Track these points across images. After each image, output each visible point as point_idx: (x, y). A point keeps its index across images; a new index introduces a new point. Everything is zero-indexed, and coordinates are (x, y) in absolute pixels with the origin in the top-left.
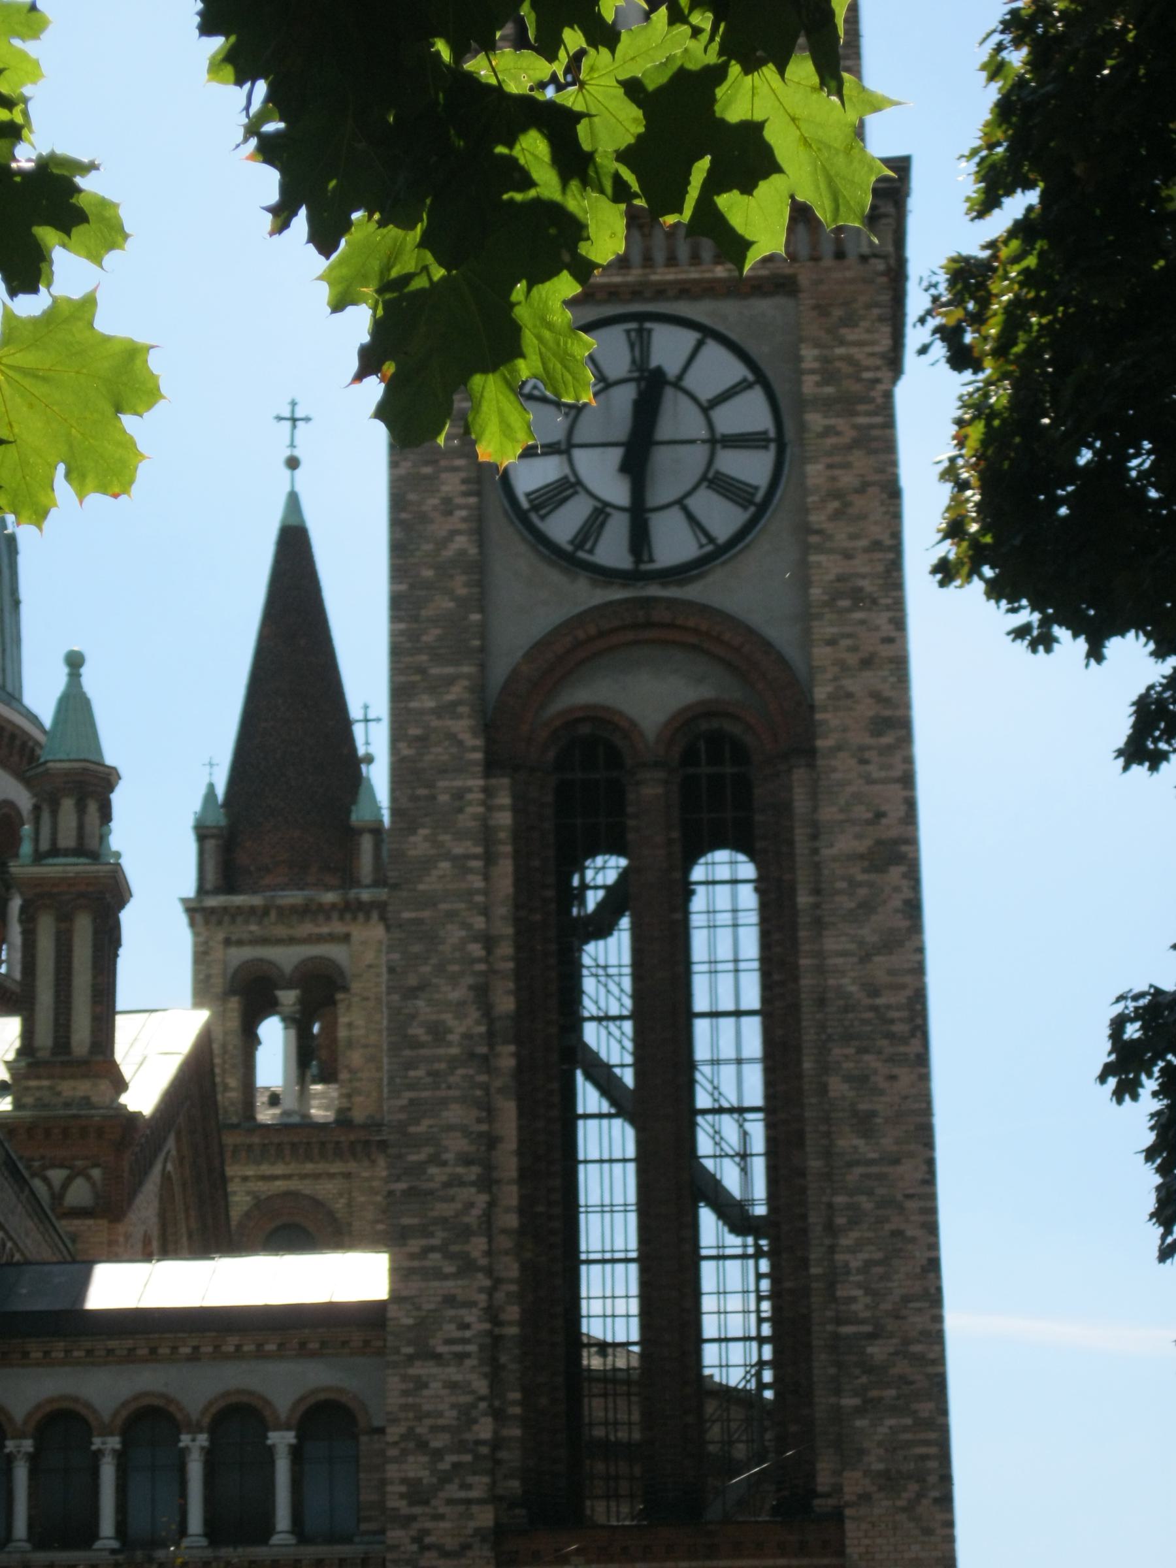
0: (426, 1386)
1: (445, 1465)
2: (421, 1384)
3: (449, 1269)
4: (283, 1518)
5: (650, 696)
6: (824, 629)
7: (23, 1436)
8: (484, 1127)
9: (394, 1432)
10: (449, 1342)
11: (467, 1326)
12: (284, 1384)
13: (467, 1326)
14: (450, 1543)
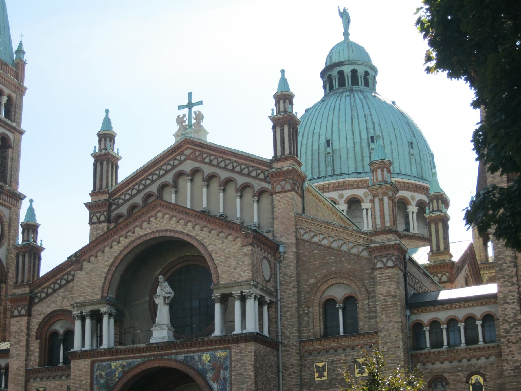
0: (506, 309)
1: (512, 325)
2: (505, 309)
3: (509, 285)
4: (481, 339)
7: (427, 326)
8: (514, 255)
9: (501, 319)
10: (511, 300)
11: (514, 296)
12: (478, 311)
13: (514, 296)
14: (514, 341)
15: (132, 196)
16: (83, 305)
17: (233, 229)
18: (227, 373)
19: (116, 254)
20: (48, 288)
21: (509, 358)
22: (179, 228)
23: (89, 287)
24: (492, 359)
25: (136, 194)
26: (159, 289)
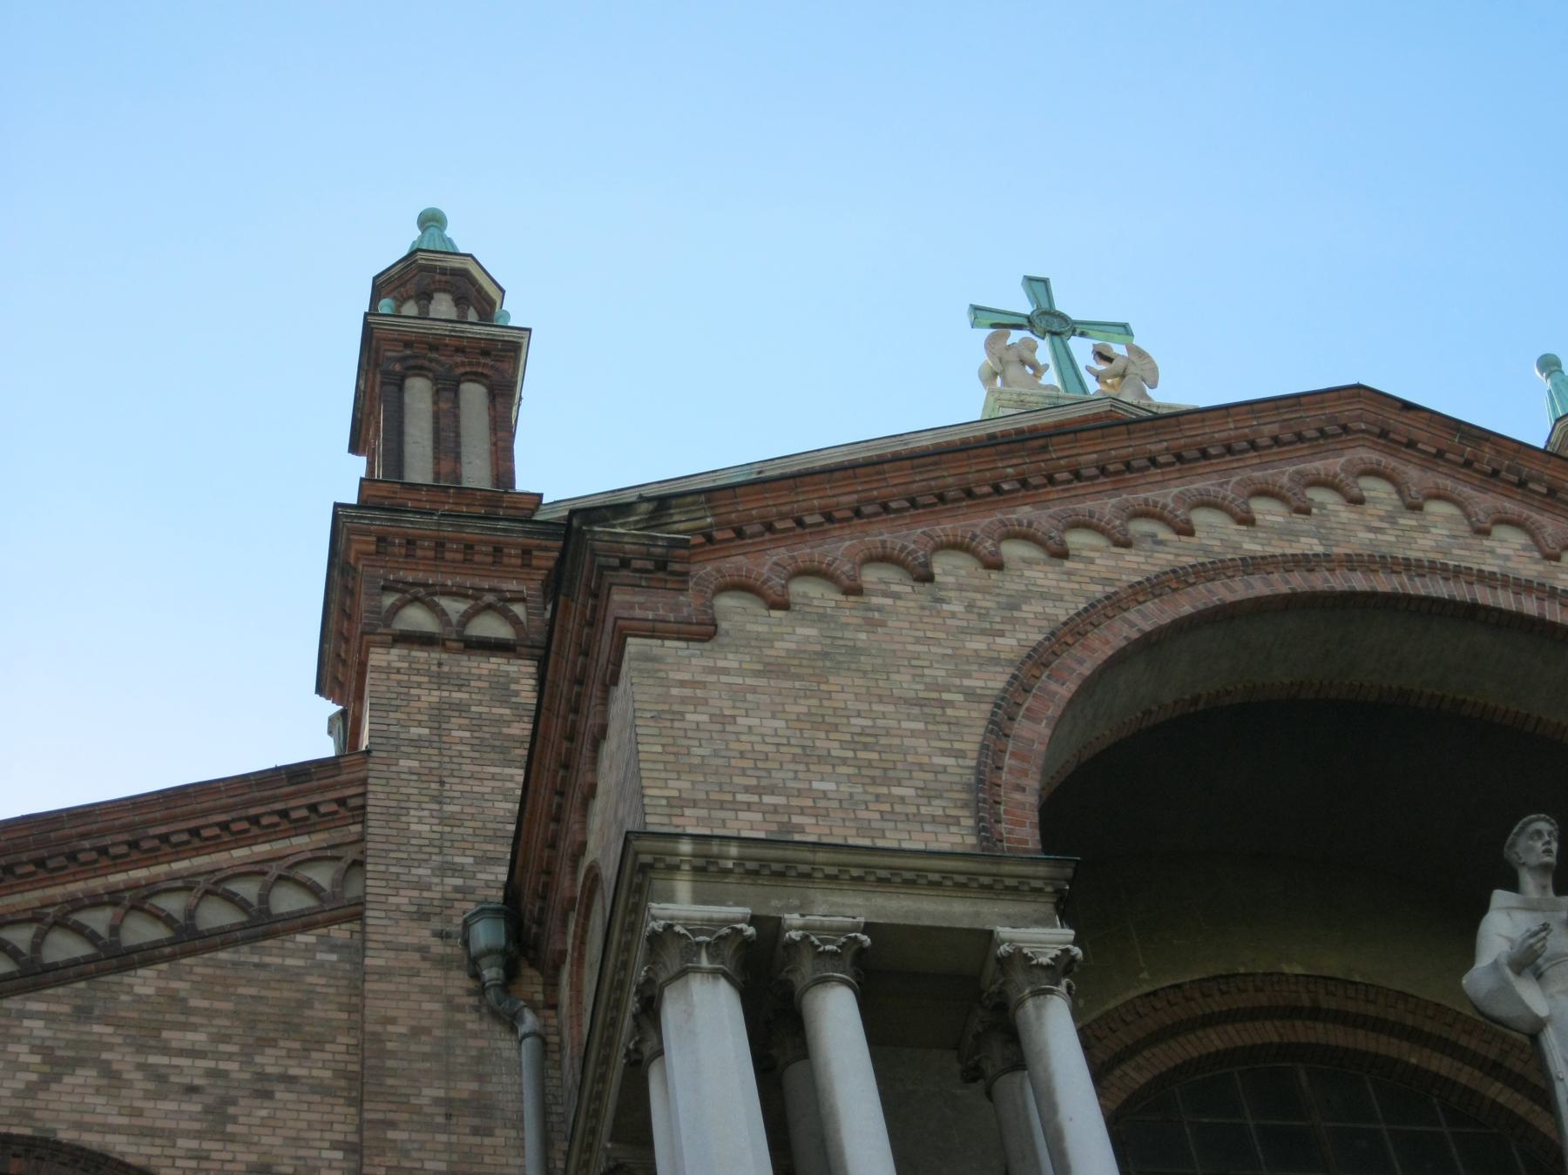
16: (779, 862)
23: (808, 757)
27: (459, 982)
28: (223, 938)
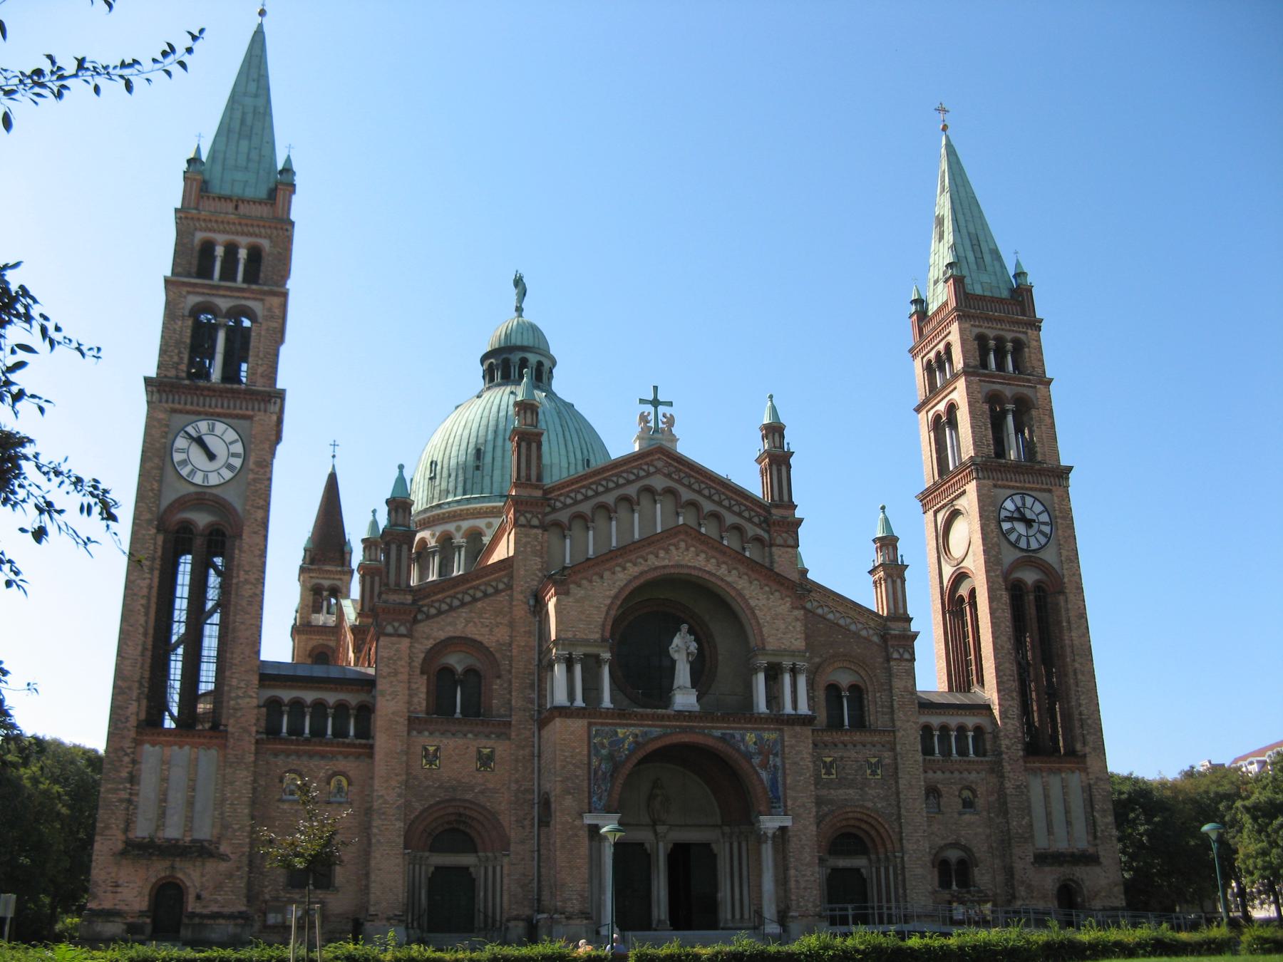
5: (1030, 577)
6: (1065, 566)
15: (576, 502)
17: (782, 585)
18: (778, 761)
19: (622, 584)
20: (442, 601)
21: (1011, 775)
22: (710, 567)
24: (983, 775)
25: (582, 501)
26: (677, 641)
27: (526, 607)
28: (491, 595)
